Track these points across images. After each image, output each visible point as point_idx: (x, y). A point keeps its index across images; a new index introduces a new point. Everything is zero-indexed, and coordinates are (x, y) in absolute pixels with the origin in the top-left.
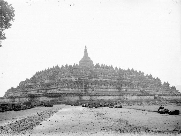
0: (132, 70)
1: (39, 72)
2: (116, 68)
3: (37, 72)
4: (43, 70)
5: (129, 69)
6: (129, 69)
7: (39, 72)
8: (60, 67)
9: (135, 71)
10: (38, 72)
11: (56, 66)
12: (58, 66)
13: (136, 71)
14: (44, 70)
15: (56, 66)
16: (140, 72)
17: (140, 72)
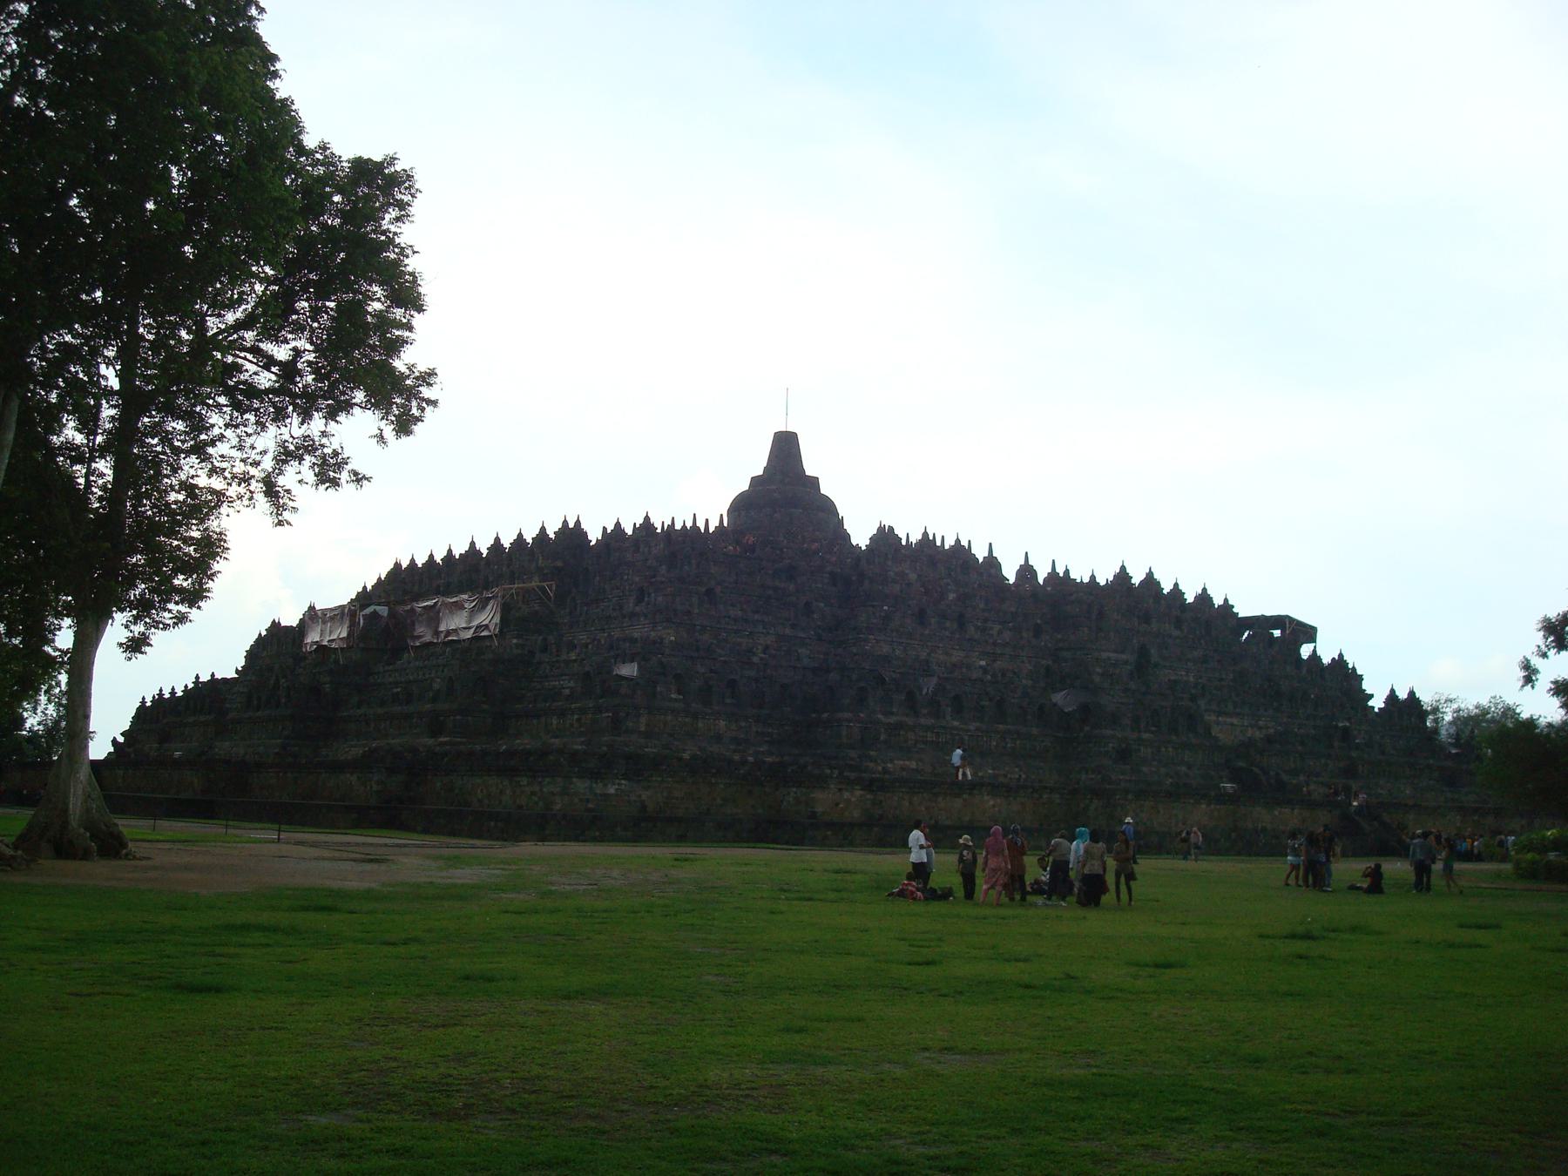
0: (1150, 581)
1: (413, 560)
2: (1026, 571)
3: (397, 565)
4: (450, 551)
5: (1123, 576)
6: (1123, 576)
7: (413, 560)
8: (594, 535)
9: (1167, 588)
10: (405, 564)
11: (565, 522)
12: (578, 523)
13: (1177, 592)
14: (460, 549)
15: (565, 522)
16: (1204, 598)
17: (1204, 598)
